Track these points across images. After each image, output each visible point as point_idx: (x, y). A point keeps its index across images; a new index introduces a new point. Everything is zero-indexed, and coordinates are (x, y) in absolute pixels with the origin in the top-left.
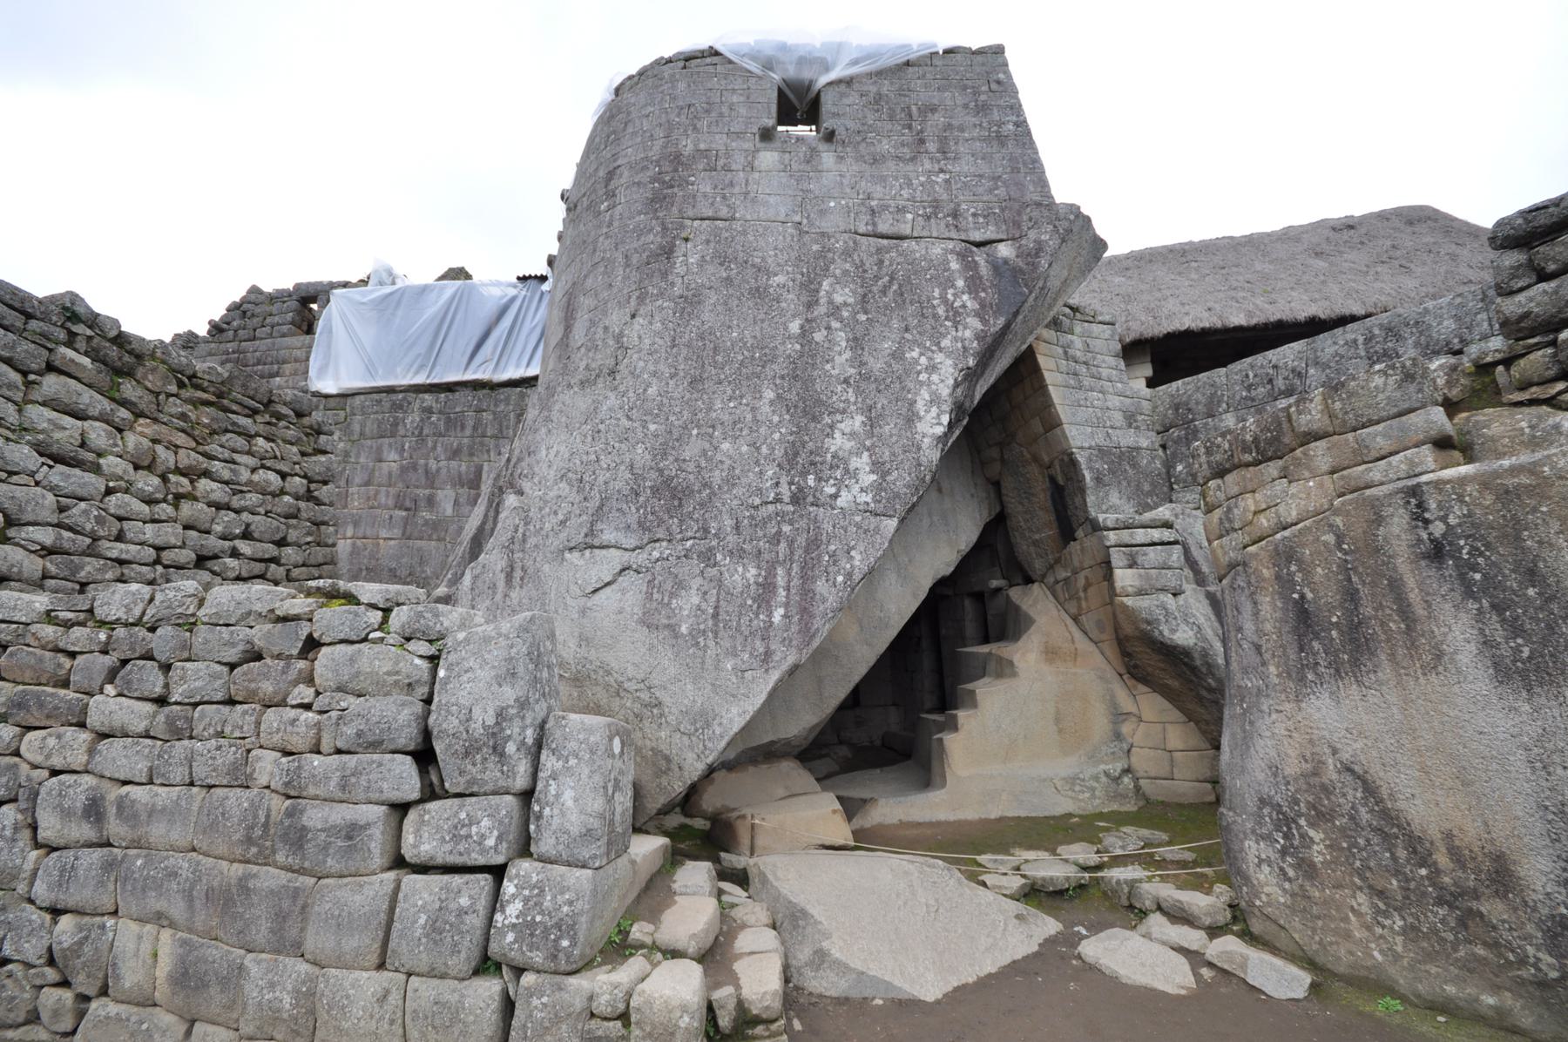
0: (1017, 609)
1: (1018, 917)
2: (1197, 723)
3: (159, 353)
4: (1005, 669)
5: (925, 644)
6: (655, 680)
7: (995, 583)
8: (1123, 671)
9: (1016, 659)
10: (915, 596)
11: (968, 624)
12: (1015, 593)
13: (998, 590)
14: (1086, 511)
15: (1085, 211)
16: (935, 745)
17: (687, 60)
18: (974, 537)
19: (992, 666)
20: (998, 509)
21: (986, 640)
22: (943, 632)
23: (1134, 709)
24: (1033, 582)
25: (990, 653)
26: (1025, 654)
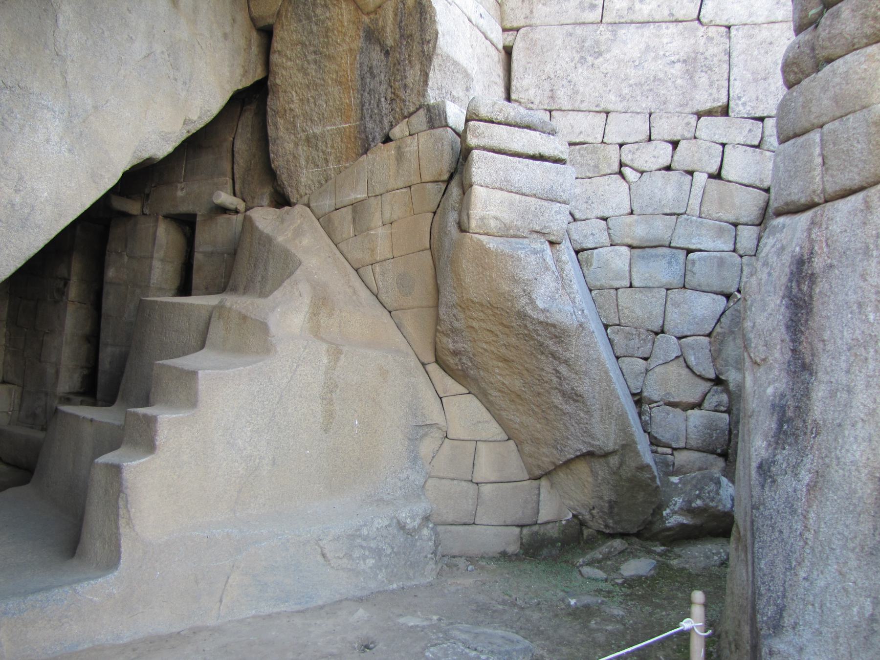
0: (267, 241)
5: (73, 291)
8: (429, 357)
9: (273, 321)
11: (157, 264)
13: (223, 210)
14: (423, 94)
16: (99, 477)
22: (111, 273)
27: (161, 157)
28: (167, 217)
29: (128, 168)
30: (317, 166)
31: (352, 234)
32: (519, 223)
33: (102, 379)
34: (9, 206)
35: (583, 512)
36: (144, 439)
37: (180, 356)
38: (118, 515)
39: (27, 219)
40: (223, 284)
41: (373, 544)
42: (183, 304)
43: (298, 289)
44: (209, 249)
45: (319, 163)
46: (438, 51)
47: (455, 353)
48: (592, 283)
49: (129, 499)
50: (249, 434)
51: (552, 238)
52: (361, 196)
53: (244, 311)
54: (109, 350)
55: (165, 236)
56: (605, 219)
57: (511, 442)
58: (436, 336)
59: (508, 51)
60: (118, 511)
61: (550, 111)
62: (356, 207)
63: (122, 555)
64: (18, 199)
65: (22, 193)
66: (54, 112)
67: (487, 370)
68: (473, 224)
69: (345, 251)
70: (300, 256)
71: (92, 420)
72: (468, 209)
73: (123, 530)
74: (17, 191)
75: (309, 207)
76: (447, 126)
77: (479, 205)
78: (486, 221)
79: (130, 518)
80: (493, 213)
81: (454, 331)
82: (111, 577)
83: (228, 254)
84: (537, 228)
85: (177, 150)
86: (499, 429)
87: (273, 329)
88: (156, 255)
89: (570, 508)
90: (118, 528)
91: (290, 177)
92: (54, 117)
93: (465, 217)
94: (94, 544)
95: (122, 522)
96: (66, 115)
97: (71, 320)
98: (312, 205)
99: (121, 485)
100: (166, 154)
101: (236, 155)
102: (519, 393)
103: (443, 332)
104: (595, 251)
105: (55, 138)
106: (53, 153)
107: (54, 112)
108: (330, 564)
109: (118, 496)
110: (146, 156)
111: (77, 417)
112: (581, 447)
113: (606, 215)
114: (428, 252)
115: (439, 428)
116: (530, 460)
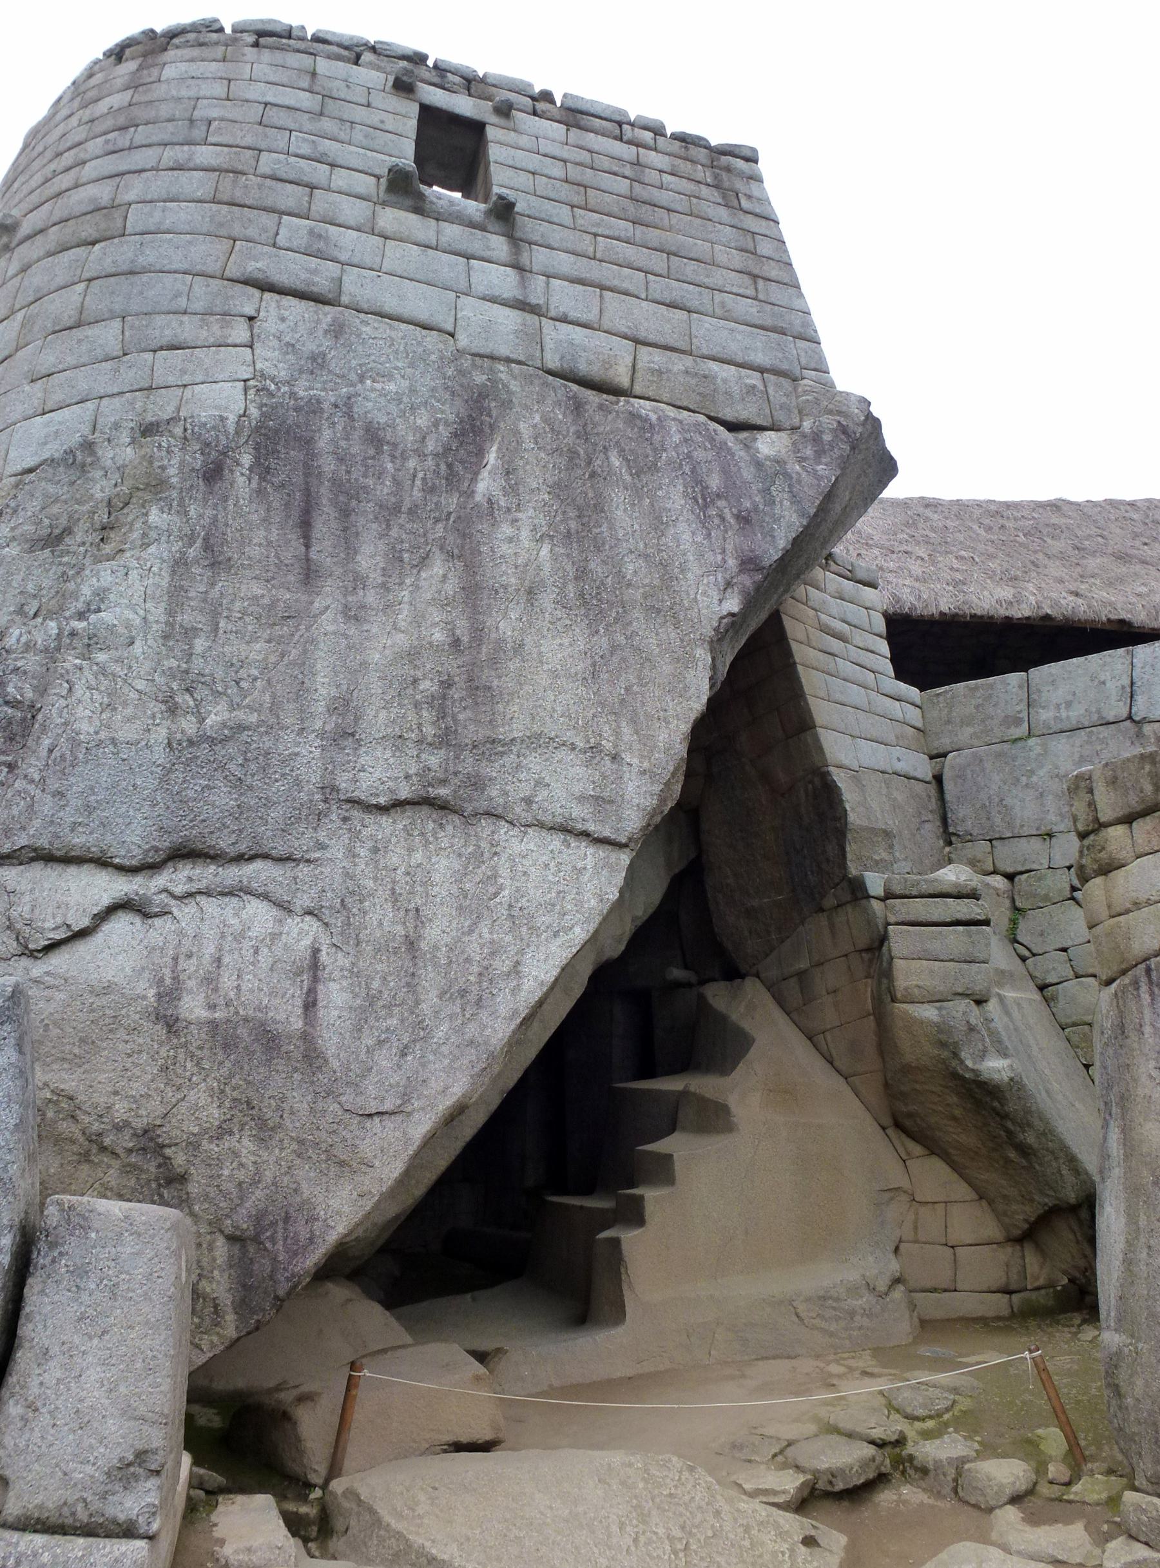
0: (722, 1019)
1: (809, 1541)
2: (990, 1203)
3: (294, 33)
4: (713, 1118)
6: (170, 1132)
8: (887, 1121)
9: (733, 1101)
12: (717, 995)
13: (678, 985)
14: (843, 865)
15: (875, 411)
17: (261, 34)
18: (656, 897)
20: (693, 856)
23: (904, 1183)
24: (742, 977)
25: (685, 1093)
26: (743, 1091)
35: (1077, 1275)
36: (634, 1215)
40: (685, 1064)
46: (850, 826)
47: (910, 1115)
48: (1063, 1021)
51: (978, 997)
52: (803, 965)
56: (1064, 950)
59: (938, 779)
61: (990, 841)
62: (801, 975)
70: (754, 1033)
73: (627, 1293)
75: (759, 977)
76: (869, 897)
84: (960, 990)
86: (970, 1189)
89: (1065, 1272)
90: (622, 1291)
95: (625, 1287)
98: (762, 975)
104: (1060, 986)
112: (1046, 1200)
113: (1065, 945)
116: (1007, 1220)
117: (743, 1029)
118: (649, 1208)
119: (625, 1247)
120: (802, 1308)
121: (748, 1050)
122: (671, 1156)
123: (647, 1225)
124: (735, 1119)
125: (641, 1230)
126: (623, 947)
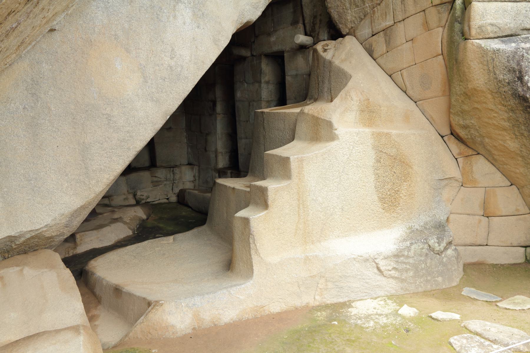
4: (321, 131)
5: (219, 108)
7: (302, 39)
8: (446, 131)
9: (335, 119)
10: (216, 42)
16: (237, 227)
19: (302, 128)
21: (282, 101)
24: (343, 36)
26: (342, 114)
27: (255, 20)
28: (267, 56)
29: (235, 31)
30: (357, 6)
31: (385, 51)
32: (512, 25)
33: (241, 159)
34: (169, 68)
37: (281, 146)
38: (250, 248)
39: (180, 75)
40: (305, 96)
41: (411, 261)
42: (280, 113)
43: (350, 96)
44: (294, 73)
45: (359, 4)
47: (465, 127)
49: (255, 238)
50: (325, 193)
53: (316, 115)
54: (244, 141)
55: (267, 69)
57: (513, 186)
58: (449, 116)
60: (250, 245)
63: (254, 271)
64: (173, 63)
65: (175, 59)
66: (185, 3)
67: (490, 138)
68: (473, 32)
69: (381, 64)
71: (234, 188)
72: (469, 21)
74: (172, 58)
77: (478, 17)
78: (484, 29)
79: (257, 250)
80: (489, 21)
81: (463, 112)
82: (249, 284)
83: (306, 75)
85: (264, 13)
87: (335, 125)
88: (263, 81)
90: (250, 255)
91: (340, 17)
92: (186, 7)
93: (466, 28)
94: (239, 264)
95: (253, 252)
96: (192, 4)
97: (220, 127)
99: (250, 230)
100: (257, 17)
101: (304, 7)
102: (518, 152)
103: (454, 114)
105: (188, 21)
106: (188, 31)
107: (185, 3)
108: (383, 274)
109: (249, 236)
110: (245, 21)
111: (226, 186)
114: (441, 57)
115: (456, 180)
117: (343, 70)
118: (271, 196)
119: (254, 224)
120: (382, 264)
121: (346, 84)
122: (288, 158)
123: (270, 207)
124: (336, 131)
125: (265, 212)
126: (259, 13)
